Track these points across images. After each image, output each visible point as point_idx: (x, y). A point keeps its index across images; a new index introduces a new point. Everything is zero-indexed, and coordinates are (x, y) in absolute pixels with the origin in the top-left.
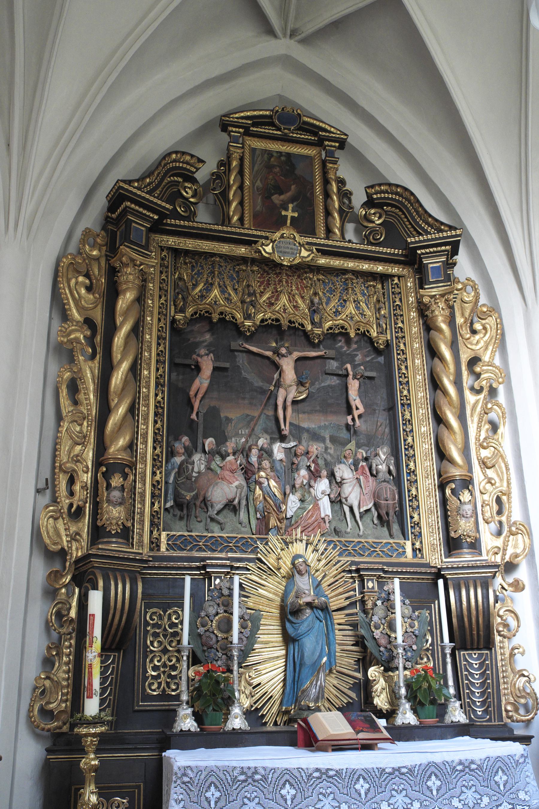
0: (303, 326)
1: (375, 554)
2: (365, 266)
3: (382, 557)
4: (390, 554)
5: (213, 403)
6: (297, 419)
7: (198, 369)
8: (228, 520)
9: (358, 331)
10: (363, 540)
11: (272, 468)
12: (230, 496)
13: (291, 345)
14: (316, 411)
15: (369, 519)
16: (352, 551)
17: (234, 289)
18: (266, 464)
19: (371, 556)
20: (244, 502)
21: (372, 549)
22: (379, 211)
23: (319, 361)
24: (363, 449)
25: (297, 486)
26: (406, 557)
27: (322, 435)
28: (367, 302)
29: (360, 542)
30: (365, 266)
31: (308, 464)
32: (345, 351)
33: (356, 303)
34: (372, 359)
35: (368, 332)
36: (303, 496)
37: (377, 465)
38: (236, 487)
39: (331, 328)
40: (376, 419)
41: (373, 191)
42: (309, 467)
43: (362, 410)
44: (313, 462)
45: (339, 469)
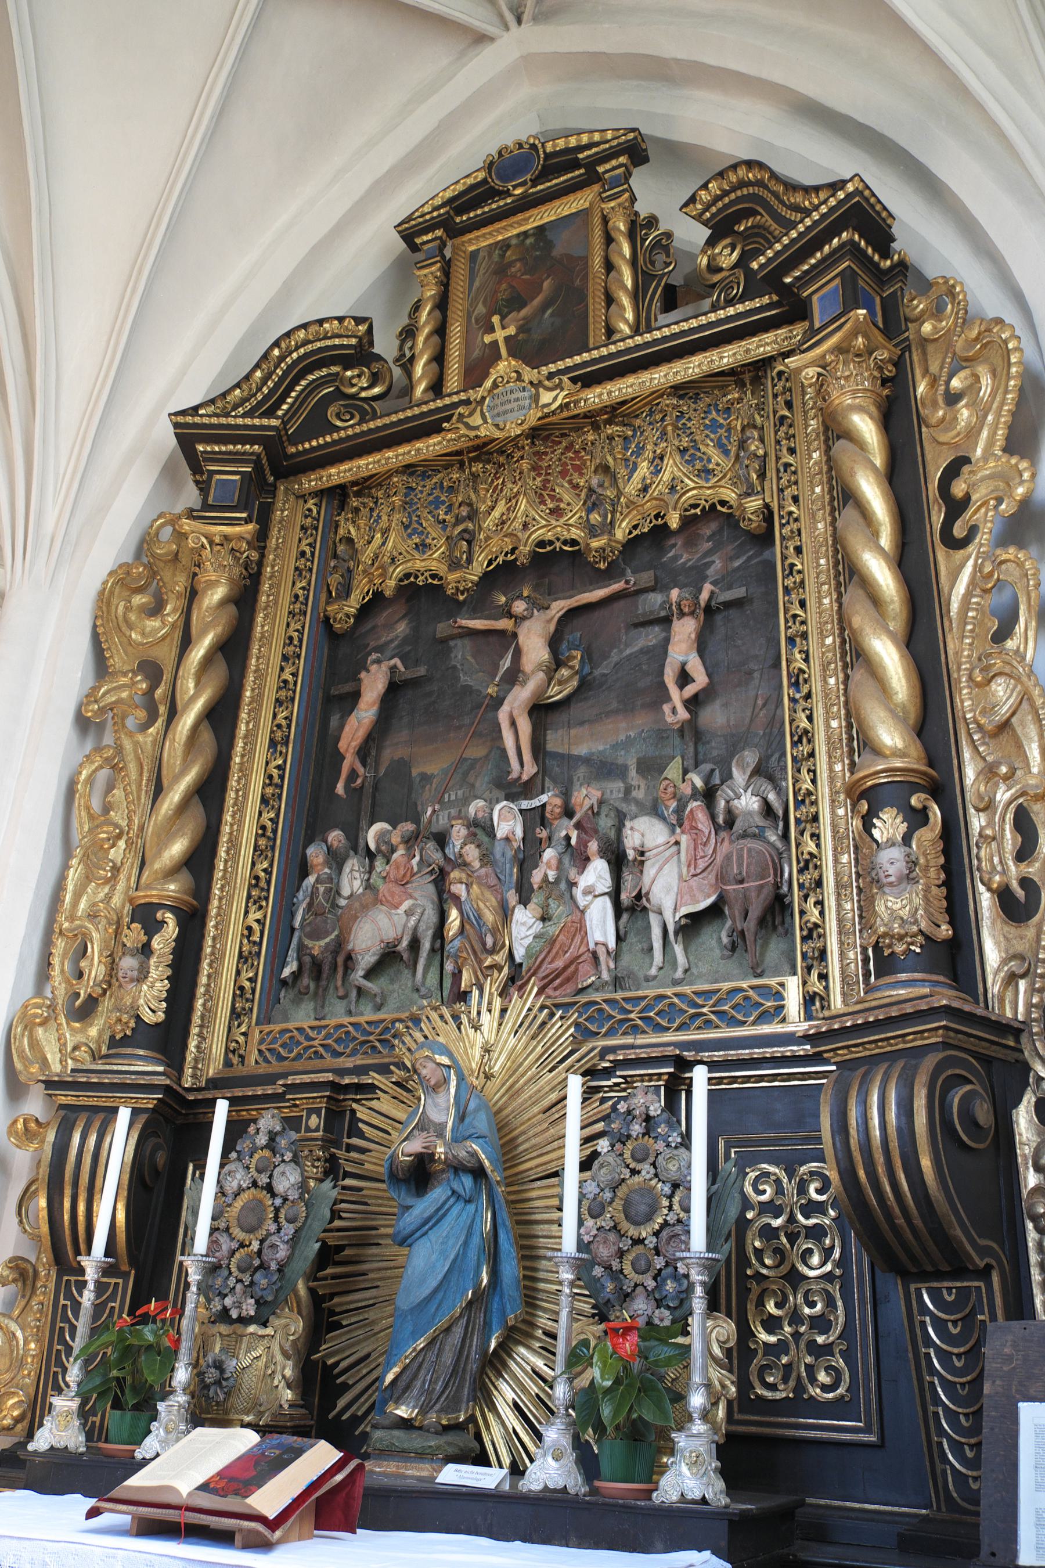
0: (574, 542)
1: (698, 1022)
2: (693, 367)
3: (717, 1027)
4: (740, 1017)
5: (401, 753)
6: (566, 740)
7: (355, 696)
8: (396, 987)
9: (693, 511)
10: (669, 992)
11: (486, 858)
12: (390, 935)
13: (536, 588)
14: (608, 714)
15: (715, 936)
16: (639, 1022)
17: (439, 522)
18: (472, 853)
19: (689, 1029)
20: (426, 945)
21: (693, 1011)
22: (728, 241)
23: (621, 604)
24: (699, 774)
25: (535, 886)
26: (783, 1020)
27: (620, 761)
28: (725, 441)
29: (661, 997)
30: (693, 367)
31: (563, 833)
32: (685, 563)
33: (692, 451)
34: (749, 559)
35: (723, 503)
36: (545, 907)
37: (728, 802)
38: (409, 913)
39: (635, 527)
40: (752, 693)
41: (699, 206)
42: (568, 838)
43: (700, 679)
44: (578, 826)
45: (632, 829)
